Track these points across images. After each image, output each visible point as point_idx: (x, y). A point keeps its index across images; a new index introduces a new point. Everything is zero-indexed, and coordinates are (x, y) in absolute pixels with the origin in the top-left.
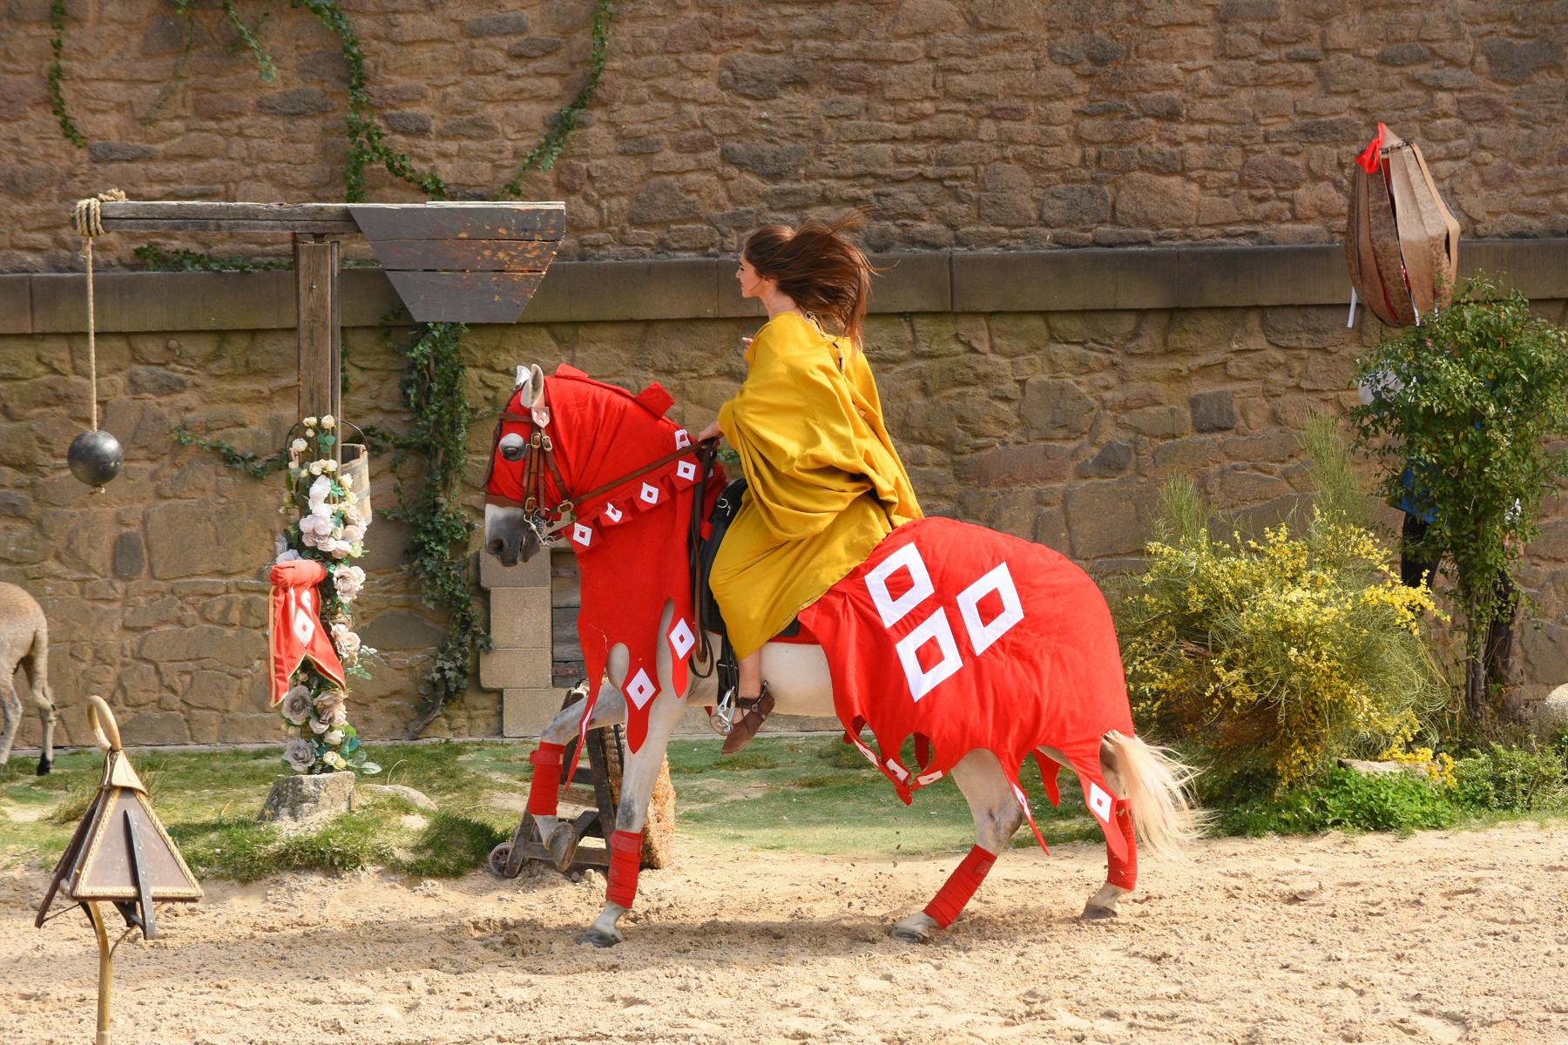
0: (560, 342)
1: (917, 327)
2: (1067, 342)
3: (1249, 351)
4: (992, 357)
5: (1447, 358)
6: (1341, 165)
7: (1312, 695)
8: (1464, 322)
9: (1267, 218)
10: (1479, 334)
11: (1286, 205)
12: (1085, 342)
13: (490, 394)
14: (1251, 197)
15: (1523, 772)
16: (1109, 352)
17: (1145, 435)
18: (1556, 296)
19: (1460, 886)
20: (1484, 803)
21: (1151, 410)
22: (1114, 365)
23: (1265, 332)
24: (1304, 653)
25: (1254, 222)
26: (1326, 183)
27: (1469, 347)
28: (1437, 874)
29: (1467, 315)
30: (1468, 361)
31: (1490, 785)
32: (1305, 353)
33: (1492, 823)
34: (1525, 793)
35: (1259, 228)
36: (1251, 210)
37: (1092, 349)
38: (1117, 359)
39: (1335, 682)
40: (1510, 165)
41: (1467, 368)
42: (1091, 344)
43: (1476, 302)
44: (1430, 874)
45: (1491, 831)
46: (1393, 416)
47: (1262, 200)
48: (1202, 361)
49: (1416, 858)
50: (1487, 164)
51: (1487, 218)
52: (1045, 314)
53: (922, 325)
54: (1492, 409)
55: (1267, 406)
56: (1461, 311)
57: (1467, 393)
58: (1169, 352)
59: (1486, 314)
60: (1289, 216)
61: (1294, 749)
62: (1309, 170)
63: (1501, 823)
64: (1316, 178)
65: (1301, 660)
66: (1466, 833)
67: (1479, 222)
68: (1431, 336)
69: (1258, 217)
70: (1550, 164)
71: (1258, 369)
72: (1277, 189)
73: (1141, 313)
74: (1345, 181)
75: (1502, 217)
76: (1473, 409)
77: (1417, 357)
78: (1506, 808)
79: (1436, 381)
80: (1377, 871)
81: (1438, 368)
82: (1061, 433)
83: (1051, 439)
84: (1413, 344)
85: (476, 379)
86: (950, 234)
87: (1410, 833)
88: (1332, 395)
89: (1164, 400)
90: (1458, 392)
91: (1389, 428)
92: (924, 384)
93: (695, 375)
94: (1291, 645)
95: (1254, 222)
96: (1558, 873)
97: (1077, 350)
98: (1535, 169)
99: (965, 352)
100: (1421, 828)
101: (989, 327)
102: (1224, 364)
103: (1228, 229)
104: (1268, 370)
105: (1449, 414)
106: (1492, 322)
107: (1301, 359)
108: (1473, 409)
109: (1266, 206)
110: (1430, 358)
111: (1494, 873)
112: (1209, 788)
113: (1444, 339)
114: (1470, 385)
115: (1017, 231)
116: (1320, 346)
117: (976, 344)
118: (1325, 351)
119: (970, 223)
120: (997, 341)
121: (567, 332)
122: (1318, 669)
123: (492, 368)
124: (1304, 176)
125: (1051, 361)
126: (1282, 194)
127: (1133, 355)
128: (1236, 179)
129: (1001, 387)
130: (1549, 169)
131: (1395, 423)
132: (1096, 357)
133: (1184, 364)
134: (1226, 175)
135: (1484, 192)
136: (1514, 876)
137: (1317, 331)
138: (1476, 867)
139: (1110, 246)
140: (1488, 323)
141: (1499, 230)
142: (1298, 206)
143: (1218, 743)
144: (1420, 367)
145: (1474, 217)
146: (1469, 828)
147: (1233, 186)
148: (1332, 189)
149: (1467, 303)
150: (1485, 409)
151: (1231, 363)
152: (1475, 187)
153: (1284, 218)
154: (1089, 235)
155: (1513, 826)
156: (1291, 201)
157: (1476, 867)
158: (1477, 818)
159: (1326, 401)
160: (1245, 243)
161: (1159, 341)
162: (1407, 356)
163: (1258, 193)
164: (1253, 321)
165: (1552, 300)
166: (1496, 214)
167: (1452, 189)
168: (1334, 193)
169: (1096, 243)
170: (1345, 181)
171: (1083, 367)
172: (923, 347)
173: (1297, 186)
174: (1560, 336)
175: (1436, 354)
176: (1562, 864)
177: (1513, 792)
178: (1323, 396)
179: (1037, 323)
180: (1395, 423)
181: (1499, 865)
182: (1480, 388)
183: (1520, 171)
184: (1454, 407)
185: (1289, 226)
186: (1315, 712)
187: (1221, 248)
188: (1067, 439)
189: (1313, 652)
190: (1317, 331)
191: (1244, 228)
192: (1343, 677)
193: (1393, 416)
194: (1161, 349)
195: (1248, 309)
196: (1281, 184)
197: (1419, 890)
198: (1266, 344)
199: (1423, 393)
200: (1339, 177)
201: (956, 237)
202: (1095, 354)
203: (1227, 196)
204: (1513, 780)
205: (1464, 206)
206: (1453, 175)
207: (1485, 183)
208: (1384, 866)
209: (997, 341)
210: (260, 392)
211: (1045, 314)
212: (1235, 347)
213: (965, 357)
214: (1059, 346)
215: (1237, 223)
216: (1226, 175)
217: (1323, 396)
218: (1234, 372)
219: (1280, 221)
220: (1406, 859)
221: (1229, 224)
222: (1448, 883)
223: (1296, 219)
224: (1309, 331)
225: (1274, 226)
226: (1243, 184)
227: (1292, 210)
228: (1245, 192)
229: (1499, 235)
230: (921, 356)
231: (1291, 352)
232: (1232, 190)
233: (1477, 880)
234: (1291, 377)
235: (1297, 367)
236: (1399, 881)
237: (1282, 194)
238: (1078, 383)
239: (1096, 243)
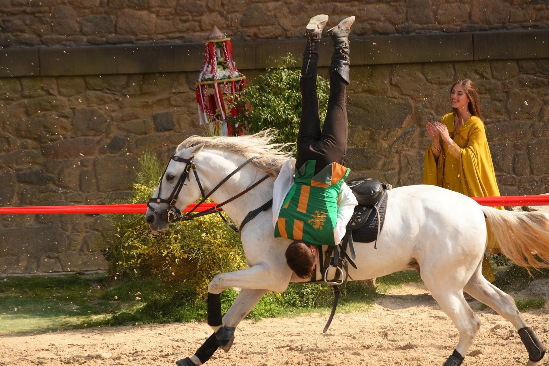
1: (24, 83)
3: (180, 93)
4: (59, 97)
5: (274, 95)
6: (223, 5)
7: (212, 255)
8: (282, 78)
9: (188, 30)
10: (289, 84)
11: (197, 23)
12: (103, 89)
14: (181, 20)
15: (312, 290)
16: (114, 94)
17: (132, 133)
18: (325, 65)
19: (283, 344)
20: (294, 304)
21: (134, 121)
22: (117, 100)
24: (209, 235)
25: (182, 32)
26: (216, 13)
27: (284, 90)
28: (272, 338)
29: (283, 74)
30: (284, 96)
31: (296, 296)
33: (298, 314)
34: (313, 300)
35: (185, 35)
36: (180, 26)
37: (106, 93)
39: (223, 248)
40: (302, 3)
41: (284, 100)
42: (106, 90)
43: (288, 69)
44: (269, 339)
45: (297, 318)
46: (249, 123)
47: (185, 21)
48: (159, 97)
49: (262, 331)
50: (291, 3)
51: (292, 29)
52: (83, 76)
53: (25, 82)
54: (296, 119)
55: (189, 119)
56: (281, 73)
57: (284, 112)
58: (143, 94)
59: (292, 74)
60: (198, 28)
61: (204, 281)
62: (208, 7)
63: (302, 314)
64: (211, 10)
65: (207, 239)
66: (286, 319)
67: (288, 31)
68: (266, 85)
69: (184, 29)
70: (321, 3)
71: (185, 101)
72: (193, 16)
74: (225, 12)
75: (299, 28)
76: (287, 119)
77: (260, 96)
78: (304, 307)
79: (269, 106)
80: (244, 338)
81: (270, 100)
82: (92, 132)
83: (87, 136)
84: (258, 89)
86: (38, 39)
87: (259, 319)
90: (280, 111)
91: (247, 128)
92: (27, 110)
94: (202, 231)
95: (182, 32)
96: (329, 337)
97: (99, 93)
98: (314, 5)
99: (46, 95)
100: (265, 317)
101: (58, 84)
102: (169, 99)
103: (170, 35)
104: (189, 102)
105: (275, 122)
106: (295, 78)
108: (287, 119)
109: (187, 25)
110: (266, 95)
111: (299, 338)
112: (165, 300)
113: (273, 86)
114: (285, 108)
115: (70, 37)
117: (51, 91)
119: (47, 34)
120: (61, 89)
122: (215, 243)
124: (205, 10)
125: (87, 99)
126: (195, 18)
128: (173, 12)
129: (63, 111)
130: (321, 5)
131: (250, 126)
132: (109, 97)
133: (150, 100)
134: (168, 10)
135: (290, 17)
136: (308, 339)
138: (291, 335)
139: (114, 44)
140: (294, 79)
141: (298, 34)
142: (203, 24)
143: (169, 278)
144: (262, 100)
145: (286, 28)
146: (287, 316)
147: (172, 14)
148: (219, 16)
149: (283, 69)
150: (292, 119)
151: (172, 99)
152: (286, 14)
153: (196, 30)
154: (104, 39)
155: (308, 315)
156: (200, 22)
157: (291, 335)
158: (291, 312)
160: (178, 42)
162: (255, 94)
163: (183, 18)
164: (182, 78)
166: (296, 27)
167: (276, 16)
168: (219, 18)
169: (107, 43)
170: (225, 12)
171: (102, 101)
172: (27, 93)
173: (202, 14)
174: (327, 84)
175: (269, 93)
176: (331, 333)
177: (308, 299)
179: (80, 81)
180: (250, 126)
181: (301, 334)
182: (289, 109)
183: (307, 6)
184: (277, 118)
185: (199, 34)
186: (214, 263)
187: (167, 44)
188: (95, 135)
189: (213, 235)
191: (177, 35)
192: (227, 246)
193: (249, 123)
195: (180, 73)
196: (195, 14)
197: (264, 346)
198: (188, 90)
199: (263, 111)
200: (222, 10)
201: (41, 41)
203: (169, 20)
204: (307, 294)
205: (281, 23)
206: (275, 9)
207: (290, 12)
208: (247, 335)
209: (61, 89)
211: (83, 76)
212: (174, 91)
213: (46, 97)
214: (91, 92)
215: (174, 32)
216: (168, 10)
218: (173, 103)
219: (194, 31)
220: (258, 332)
221: (170, 33)
222: (278, 342)
223: (202, 30)
225: (191, 33)
226: (177, 14)
227: (200, 26)
228: (178, 18)
229: (298, 37)
230: (25, 97)
232: (171, 17)
233: (291, 341)
236: (254, 342)
237: (195, 18)
238: (100, 109)
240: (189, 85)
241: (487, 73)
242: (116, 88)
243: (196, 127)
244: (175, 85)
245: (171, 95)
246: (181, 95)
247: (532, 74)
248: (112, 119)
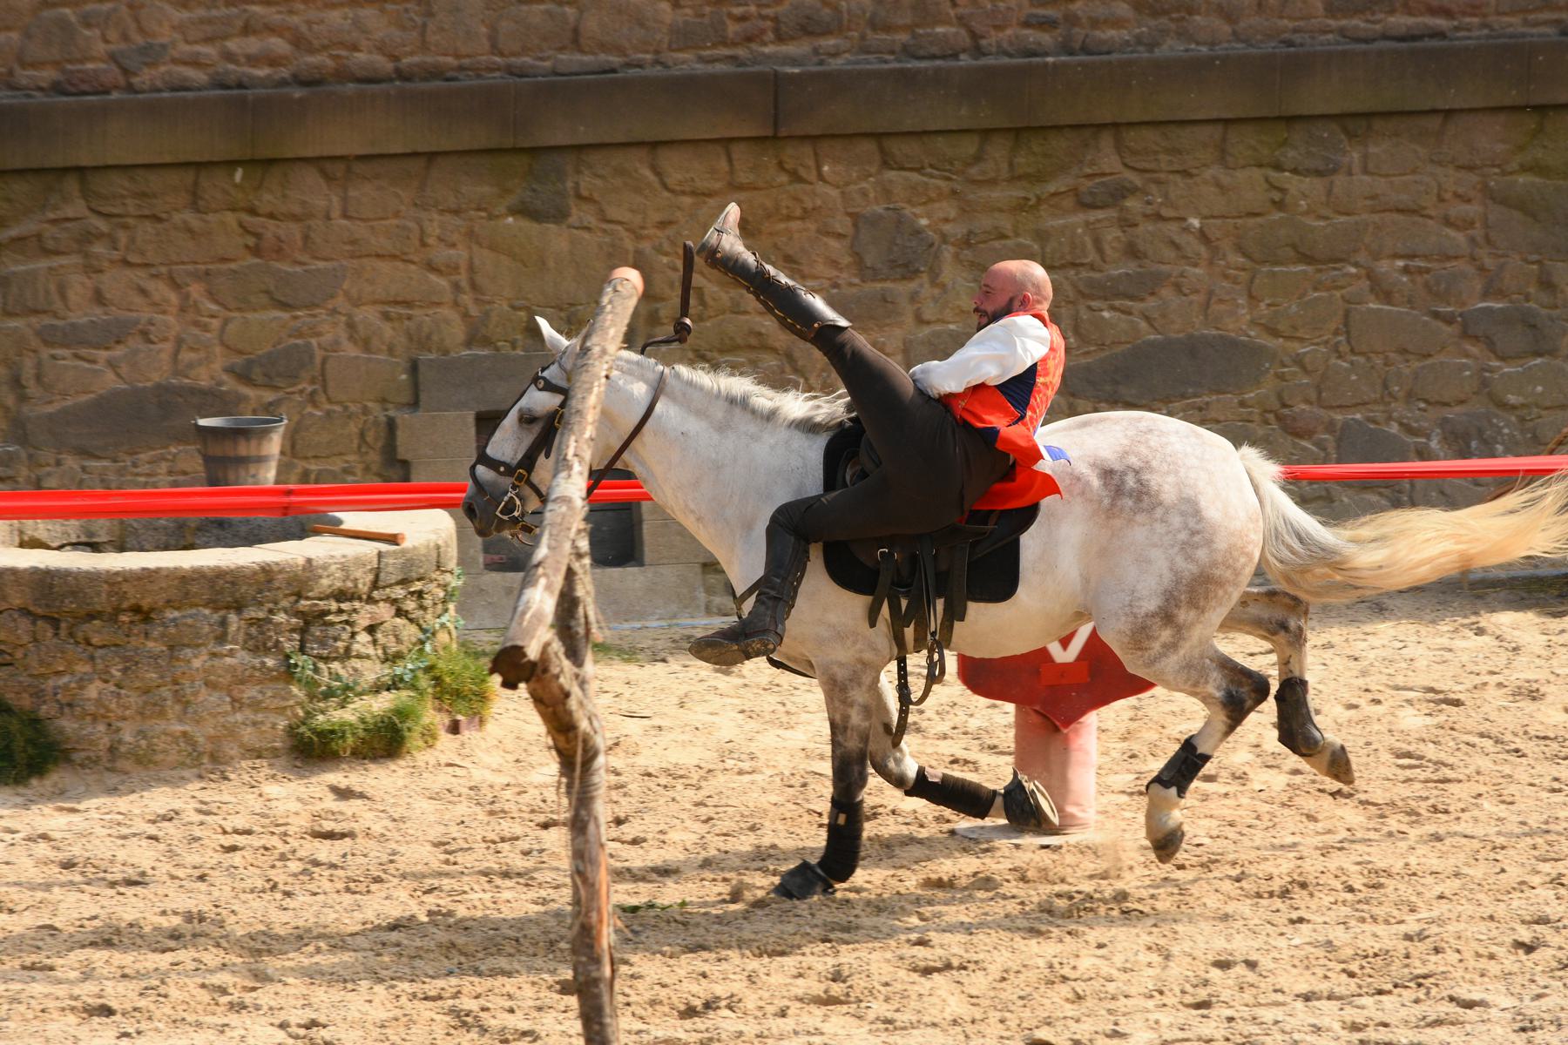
0: (328, 178)
1: (735, 156)
2: (902, 168)
12: (923, 168)
13: (1277, 196)
16: (949, 179)
23: (85, 197)
32: (131, 221)
38: (959, 188)
42: (929, 170)
48: (14, 232)
52: (878, 136)
53: (738, 151)
73: (986, 133)
85: (235, 225)
86: (1227, 29)
88: (163, 270)
89: (1011, 234)
93: (483, 214)
97: (915, 177)
99: (791, 182)
107: (125, 227)
116: (1181, 168)
117: (802, 172)
118: (156, 219)
121: (338, 169)
123: (253, 211)
127: (974, 182)
137: (144, 195)
139: (1366, 41)
154: (1378, 27)
159: (155, 276)
161: (1004, 166)
165: (415, 155)
169: (1385, 37)
178: (153, 271)
179: (868, 147)
190: (144, 195)
194: (1005, 173)
201: (1234, 33)
202: (933, 181)
210: (1027, 199)
211: (878, 136)
214: (893, 173)
217: (153, 271)
224: (1168, 151)
231: (1148, 175)
234: (116, 249)
235: (122, 236)
239: (1385, 37)
240: (1122, 157)
241: (807, 167)
242: (951, 164)
243: (105, 305)
244: (52, 202)
245: (45, 225)
246: (68, 225)
247: (911, 170)
248: (944, 238)
